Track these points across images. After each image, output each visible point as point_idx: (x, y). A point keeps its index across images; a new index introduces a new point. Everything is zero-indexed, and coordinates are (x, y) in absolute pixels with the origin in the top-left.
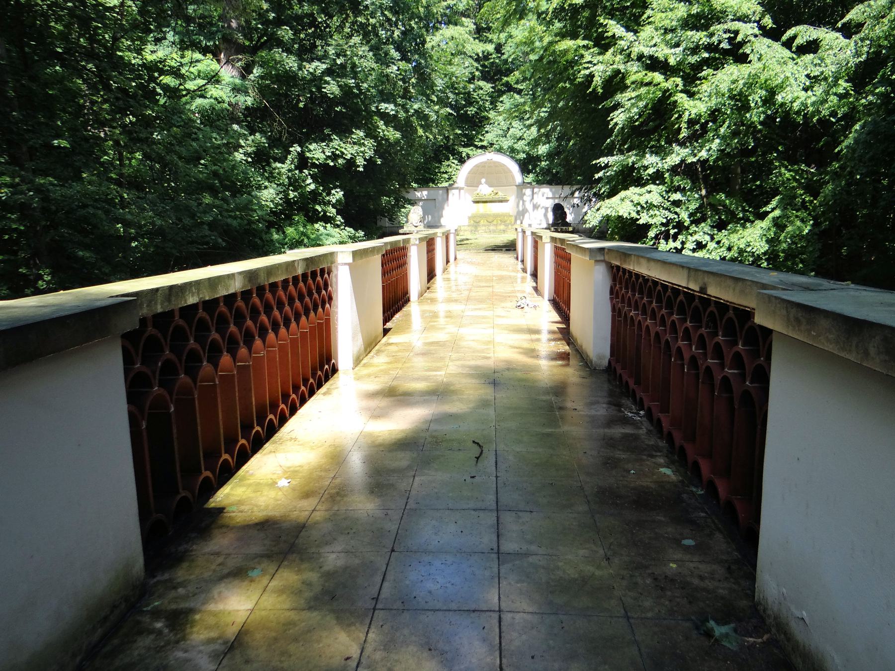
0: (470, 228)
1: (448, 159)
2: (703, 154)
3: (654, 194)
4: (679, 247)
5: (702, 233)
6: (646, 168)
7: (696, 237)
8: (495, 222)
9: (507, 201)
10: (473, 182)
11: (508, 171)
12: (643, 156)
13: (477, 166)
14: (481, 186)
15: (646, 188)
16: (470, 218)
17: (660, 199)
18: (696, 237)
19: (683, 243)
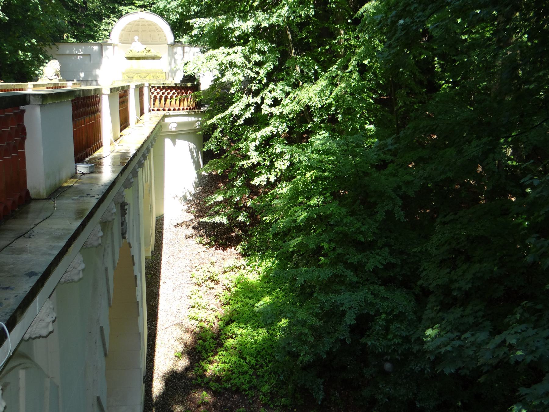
1: (109, 17)
2: (274, 19)
3: (237, 55)
4: (259, 103)
5: (277, 90)
6: (233, 30)
7: (274, 94)
10: (126, 40)
12: (232, 20)
13: (131, 24)
14: (134, 43)
16: (123, 74)
17: (243, 60)
18: (274, 94)
19: (263, 99)
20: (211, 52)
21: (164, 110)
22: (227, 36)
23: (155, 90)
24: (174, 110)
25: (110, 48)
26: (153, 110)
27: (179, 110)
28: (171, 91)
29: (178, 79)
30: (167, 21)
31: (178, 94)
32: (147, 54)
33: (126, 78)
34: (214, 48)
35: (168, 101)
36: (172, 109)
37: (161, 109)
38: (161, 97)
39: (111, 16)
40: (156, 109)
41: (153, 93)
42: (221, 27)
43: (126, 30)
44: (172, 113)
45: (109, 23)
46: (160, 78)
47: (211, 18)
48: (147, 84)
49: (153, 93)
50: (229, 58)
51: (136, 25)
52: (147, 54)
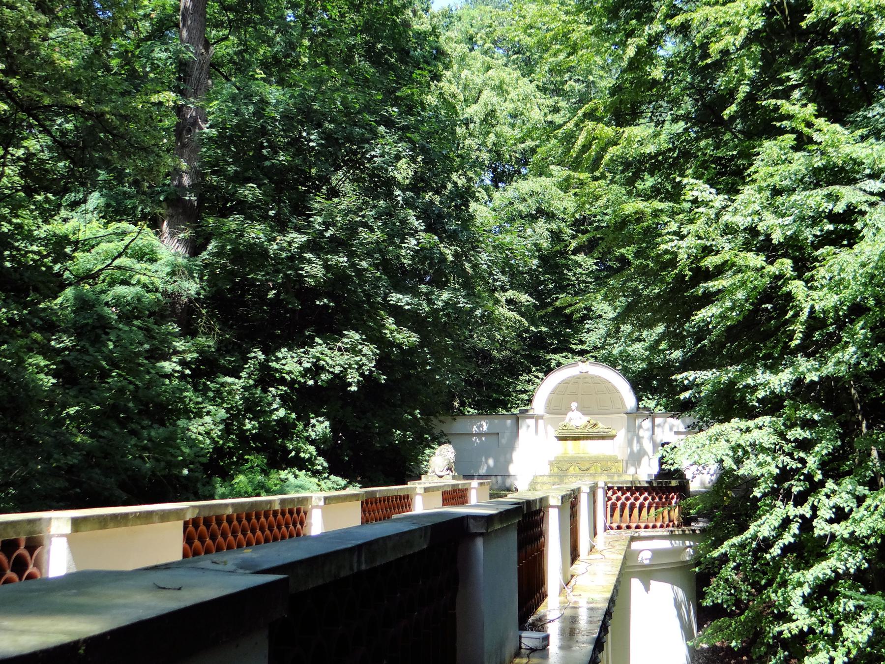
0: (551, 480)
1: (530, 372)
2: (829, 368)
3: (762, 431)
4: (808, 516)
5: (841, 493)
6: (754, 389)
7: (835, 500)
8: (592, 471)
9: (612, 437)
10: (557, 408)
12: (752, 373)
13: (565, 383)
14: (570, 414)
15: (756, 420)
16: (551, 464)
17: (775, 439)
18: (835, 500)
19: (814, 509)
20: (716, 428)
21: (628, 527)
22: (743, 398)
23: (614, 493)
24: (646, 527)
25: (531, 422)
26: (611, 528)
27: (654, 527)
28: (641, 495)
29: (647, 471)
30: (624, 375)
31: (653, 499)
32: (591, 430)
33: (556, 469)
34: (721, 422)
35: (636, 511)
36: (643, 525)
37: (624, 525)
38: (623, 506)
39: (534, 369)
40: (614, 525)
42: (732, 383)
44: (643, 532)
45: (529, 381)
46: (614, 470)
47: (714, 370)
48: (601, 484)
49: (610, 499)
50: (748, 438)
52: (591, 430)
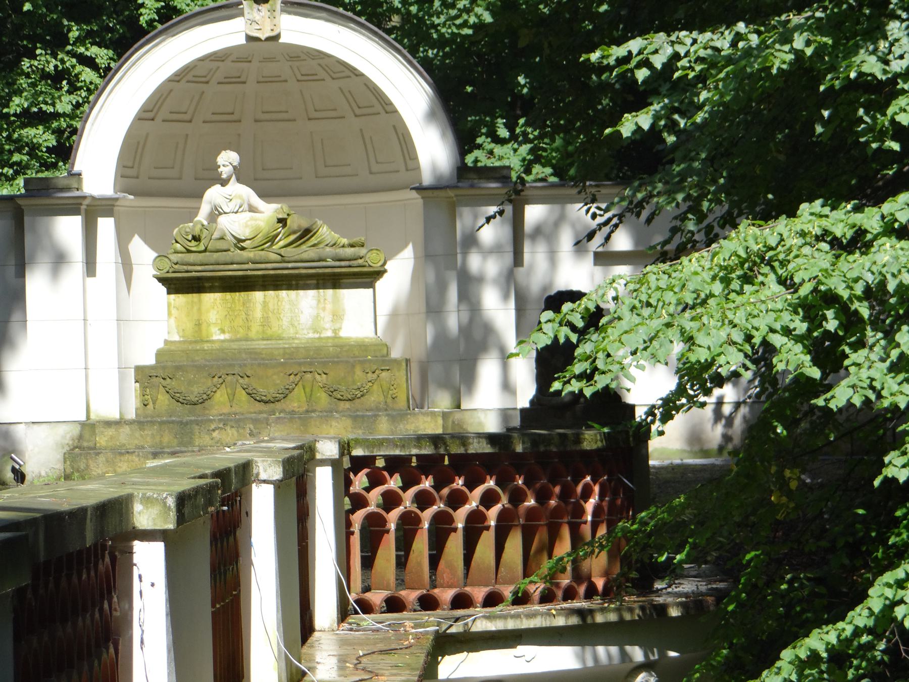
0: (147, 438)
8: (297, 402)
9: (368, 278)
11: (379, 105)
13: (189, 76)
14: (214, 194)
20: (747, 237)
21: (428, 603)
22: (845, 125)
23: (375, 480)
24: (492, 600)
25: (67, 229)
26: (366, 607)
27: (521, 599)
28: (471, 485)
30: (413, 51)
31: (517, 497)
32: (290, 252)
33: (163, 399)
34: (767, 215)
35: (455, 545)
36: (479, 593)
37: (411, 596)
38: (409, 523)
39: (74, 34)
40: (377, 597)
41: (359, 502)
42: (804, 70)
43: (163, 113)
44: (482, 622)
45: (57, 77)
46: (375, 398)
47: (741, 27)
48: (328, 449)
49: (359, 502)
50: (860, 268)
51: (229, 80)
52: (290, 252)
